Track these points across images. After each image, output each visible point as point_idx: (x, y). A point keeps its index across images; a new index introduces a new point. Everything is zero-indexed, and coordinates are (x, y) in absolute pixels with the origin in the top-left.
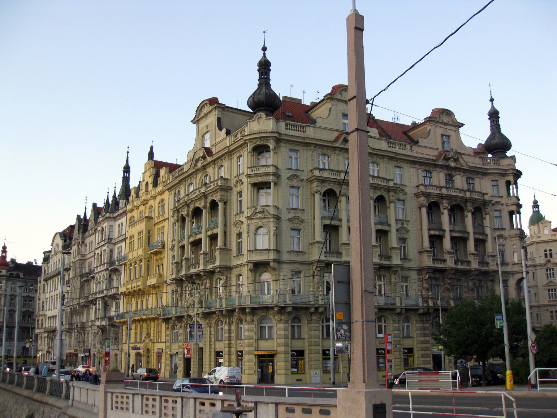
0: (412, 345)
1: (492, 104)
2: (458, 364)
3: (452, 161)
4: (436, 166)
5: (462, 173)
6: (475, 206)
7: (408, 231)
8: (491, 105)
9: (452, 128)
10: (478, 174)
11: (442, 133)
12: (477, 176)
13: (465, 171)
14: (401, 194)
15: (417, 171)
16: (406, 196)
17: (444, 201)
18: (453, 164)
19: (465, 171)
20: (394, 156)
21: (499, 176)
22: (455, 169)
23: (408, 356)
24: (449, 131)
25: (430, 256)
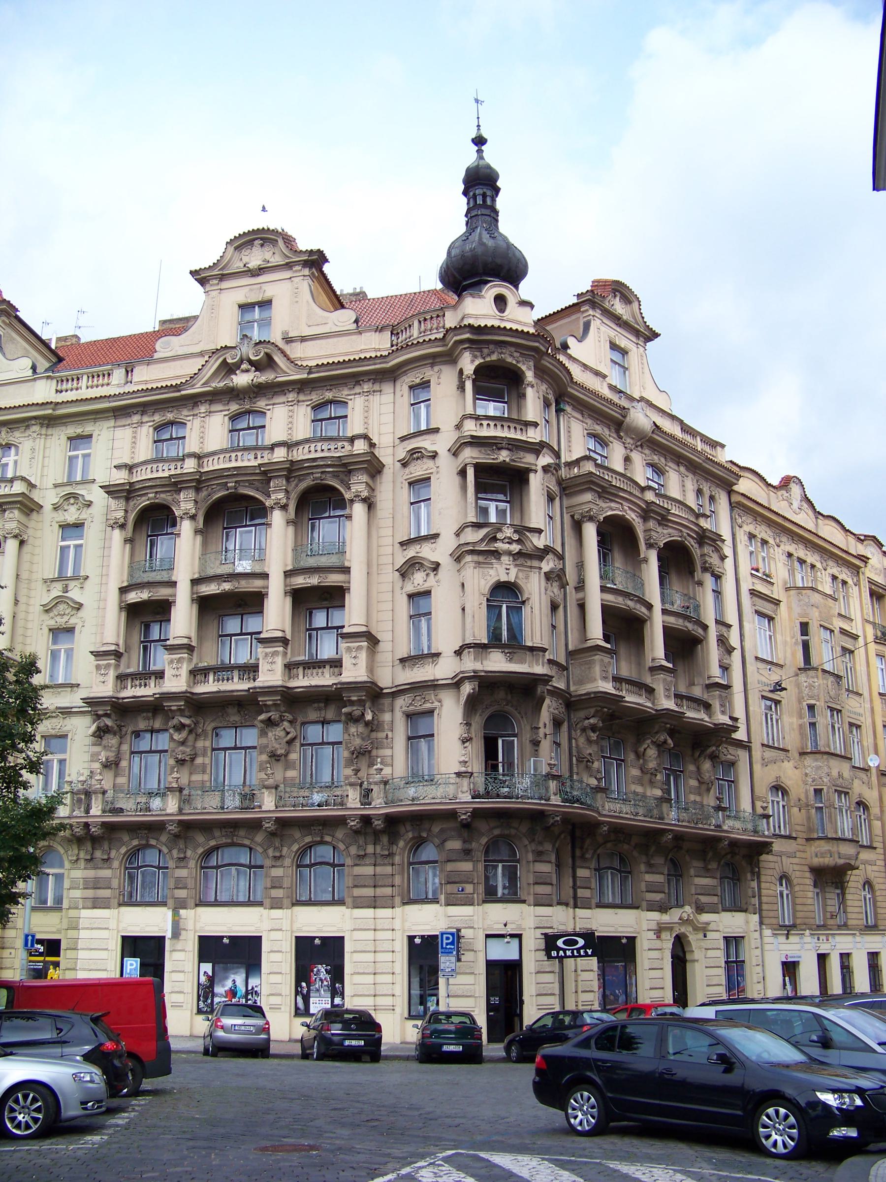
0: (59, 931)
1: (480, 151)
2: (217, 1000)
3: (247, 371)
4: (194, 400)
5: (291, 396)
6: (303, 485)
7: (79, 607)
8: (476, 155)
9: (287, 274)
10: (358, 383)
11: (242, 300)
12: (358, 390)
13: (302, 386)
14: (73, 509)
15: (135, 432)
16: (90, 510)
17: (182, 495)
18: (242, 379)
19: (302, 386)
20: (50, 411)
21: (432, 365)
22: (258, 390)
23: (46, 965)
24: (264, 287)
25: (108, 665)
